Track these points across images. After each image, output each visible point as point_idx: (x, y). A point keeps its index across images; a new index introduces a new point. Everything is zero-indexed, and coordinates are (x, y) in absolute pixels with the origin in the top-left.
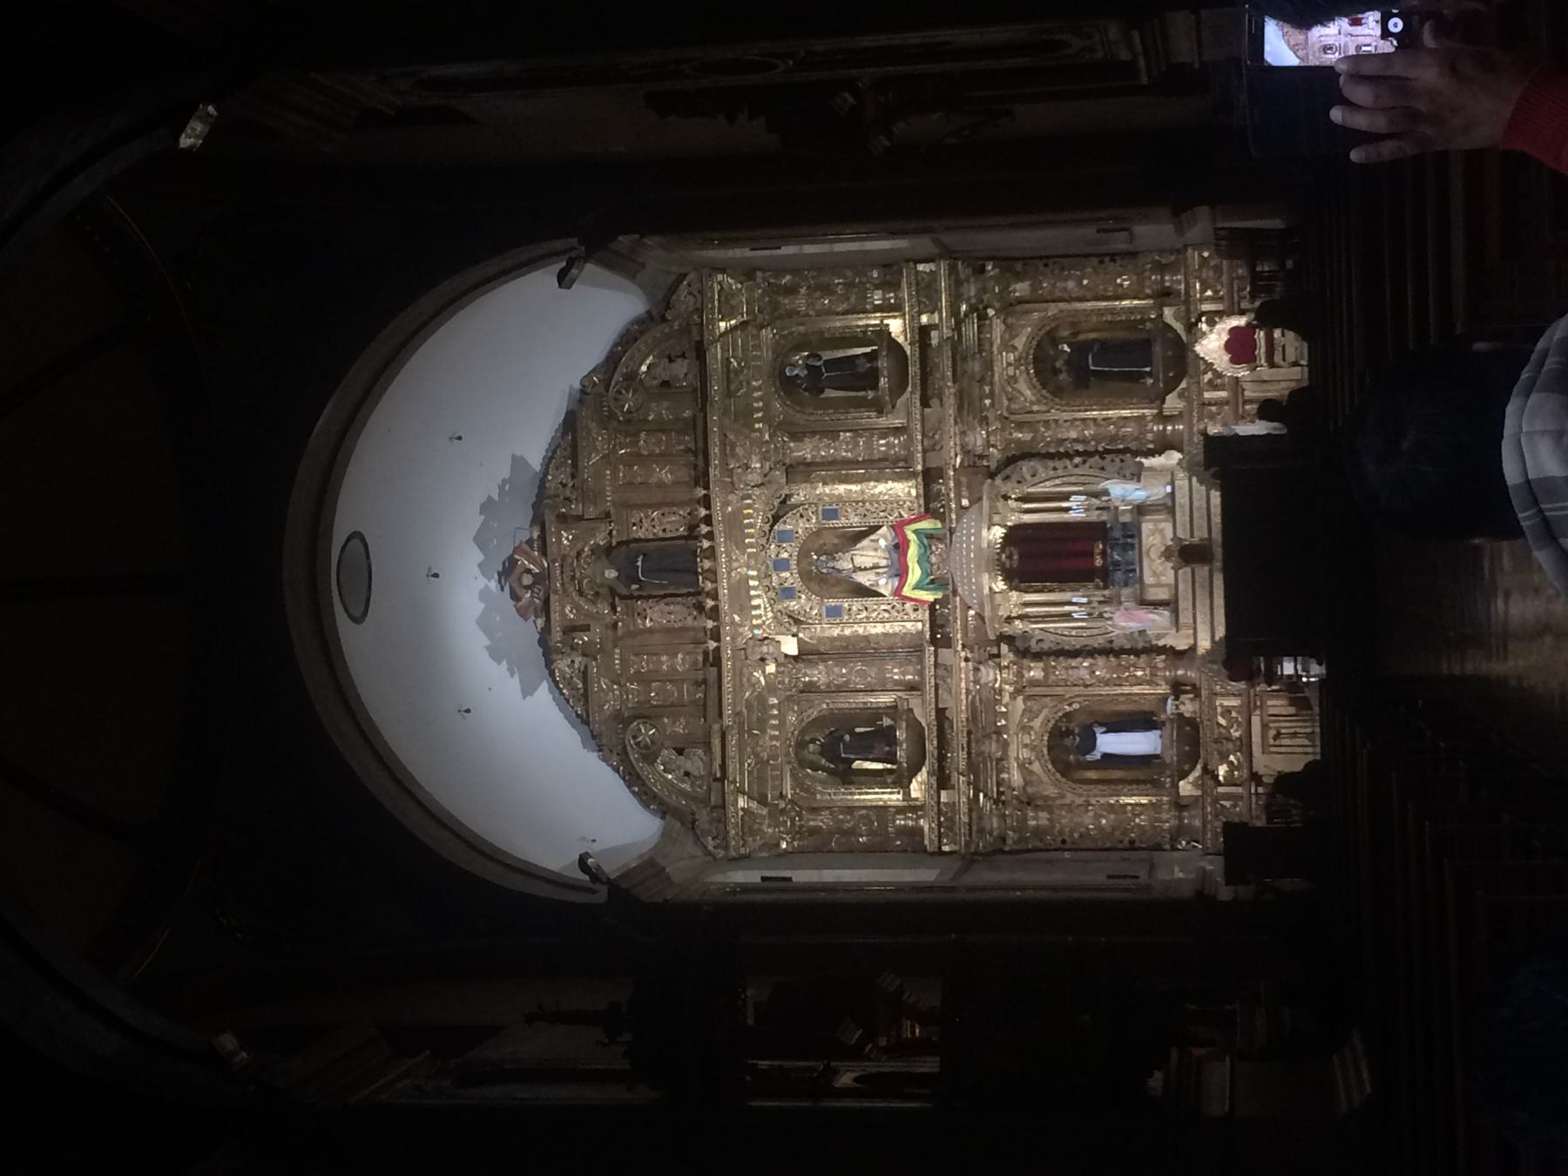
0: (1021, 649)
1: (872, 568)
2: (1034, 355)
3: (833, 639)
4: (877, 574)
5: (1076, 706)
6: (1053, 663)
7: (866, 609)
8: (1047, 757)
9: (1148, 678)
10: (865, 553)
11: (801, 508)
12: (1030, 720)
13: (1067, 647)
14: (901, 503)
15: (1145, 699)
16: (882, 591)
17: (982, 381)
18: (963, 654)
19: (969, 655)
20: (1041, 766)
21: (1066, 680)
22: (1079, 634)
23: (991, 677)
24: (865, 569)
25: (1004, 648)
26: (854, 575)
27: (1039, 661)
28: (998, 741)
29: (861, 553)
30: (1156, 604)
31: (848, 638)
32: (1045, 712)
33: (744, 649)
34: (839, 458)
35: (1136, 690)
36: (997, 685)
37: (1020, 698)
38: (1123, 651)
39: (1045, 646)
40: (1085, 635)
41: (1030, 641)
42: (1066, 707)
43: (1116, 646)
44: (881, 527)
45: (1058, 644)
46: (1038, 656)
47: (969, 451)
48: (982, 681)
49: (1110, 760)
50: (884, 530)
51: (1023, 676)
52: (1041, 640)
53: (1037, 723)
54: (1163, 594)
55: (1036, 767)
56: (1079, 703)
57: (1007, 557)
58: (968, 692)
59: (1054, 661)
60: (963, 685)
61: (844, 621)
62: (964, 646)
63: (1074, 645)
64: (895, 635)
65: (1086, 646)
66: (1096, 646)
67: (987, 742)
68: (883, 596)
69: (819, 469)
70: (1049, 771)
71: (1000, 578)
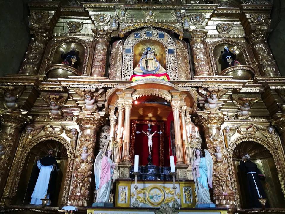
0: (103, 128)
2: (253, 141)
3: (116, 53)
4: (144, 67)
5: (69, 155)
6: (91, 140)
8: (46, 139)
10: (154, 63)
11: (173, 41)
12: (66, 131)
14: (177, 76)
16: (137, 68)
17: (237, 116)
18: (100, 87)
19: (100, 92)
20: (42, 136)
24: (146, 63)
25: (102, 114)
28: (57, 114)
30: (114, 191)
31: (116, 57)
32: (69, 140)
33: (115, 15)
34: (195, 56)
37: (77, 127)
39: (103, 140)
41: (106, 132)
42: (70, 150)
44: (166, 69)
45: (103, 146)
46: (98, 133)
47: (206, 101)
49: (37, 172)
52: (106, 138)
53: (64, 135)
54: (122, 199)
55: (43, 133)
56: (71, 157)
57: (150, 118)
59: (93, 141)
61: (124, 54)
64: (116, 74)
67: (57, 107)
68: (134, 69)
69: (189, 53)
70: (38, 140)
71: (141, 96)
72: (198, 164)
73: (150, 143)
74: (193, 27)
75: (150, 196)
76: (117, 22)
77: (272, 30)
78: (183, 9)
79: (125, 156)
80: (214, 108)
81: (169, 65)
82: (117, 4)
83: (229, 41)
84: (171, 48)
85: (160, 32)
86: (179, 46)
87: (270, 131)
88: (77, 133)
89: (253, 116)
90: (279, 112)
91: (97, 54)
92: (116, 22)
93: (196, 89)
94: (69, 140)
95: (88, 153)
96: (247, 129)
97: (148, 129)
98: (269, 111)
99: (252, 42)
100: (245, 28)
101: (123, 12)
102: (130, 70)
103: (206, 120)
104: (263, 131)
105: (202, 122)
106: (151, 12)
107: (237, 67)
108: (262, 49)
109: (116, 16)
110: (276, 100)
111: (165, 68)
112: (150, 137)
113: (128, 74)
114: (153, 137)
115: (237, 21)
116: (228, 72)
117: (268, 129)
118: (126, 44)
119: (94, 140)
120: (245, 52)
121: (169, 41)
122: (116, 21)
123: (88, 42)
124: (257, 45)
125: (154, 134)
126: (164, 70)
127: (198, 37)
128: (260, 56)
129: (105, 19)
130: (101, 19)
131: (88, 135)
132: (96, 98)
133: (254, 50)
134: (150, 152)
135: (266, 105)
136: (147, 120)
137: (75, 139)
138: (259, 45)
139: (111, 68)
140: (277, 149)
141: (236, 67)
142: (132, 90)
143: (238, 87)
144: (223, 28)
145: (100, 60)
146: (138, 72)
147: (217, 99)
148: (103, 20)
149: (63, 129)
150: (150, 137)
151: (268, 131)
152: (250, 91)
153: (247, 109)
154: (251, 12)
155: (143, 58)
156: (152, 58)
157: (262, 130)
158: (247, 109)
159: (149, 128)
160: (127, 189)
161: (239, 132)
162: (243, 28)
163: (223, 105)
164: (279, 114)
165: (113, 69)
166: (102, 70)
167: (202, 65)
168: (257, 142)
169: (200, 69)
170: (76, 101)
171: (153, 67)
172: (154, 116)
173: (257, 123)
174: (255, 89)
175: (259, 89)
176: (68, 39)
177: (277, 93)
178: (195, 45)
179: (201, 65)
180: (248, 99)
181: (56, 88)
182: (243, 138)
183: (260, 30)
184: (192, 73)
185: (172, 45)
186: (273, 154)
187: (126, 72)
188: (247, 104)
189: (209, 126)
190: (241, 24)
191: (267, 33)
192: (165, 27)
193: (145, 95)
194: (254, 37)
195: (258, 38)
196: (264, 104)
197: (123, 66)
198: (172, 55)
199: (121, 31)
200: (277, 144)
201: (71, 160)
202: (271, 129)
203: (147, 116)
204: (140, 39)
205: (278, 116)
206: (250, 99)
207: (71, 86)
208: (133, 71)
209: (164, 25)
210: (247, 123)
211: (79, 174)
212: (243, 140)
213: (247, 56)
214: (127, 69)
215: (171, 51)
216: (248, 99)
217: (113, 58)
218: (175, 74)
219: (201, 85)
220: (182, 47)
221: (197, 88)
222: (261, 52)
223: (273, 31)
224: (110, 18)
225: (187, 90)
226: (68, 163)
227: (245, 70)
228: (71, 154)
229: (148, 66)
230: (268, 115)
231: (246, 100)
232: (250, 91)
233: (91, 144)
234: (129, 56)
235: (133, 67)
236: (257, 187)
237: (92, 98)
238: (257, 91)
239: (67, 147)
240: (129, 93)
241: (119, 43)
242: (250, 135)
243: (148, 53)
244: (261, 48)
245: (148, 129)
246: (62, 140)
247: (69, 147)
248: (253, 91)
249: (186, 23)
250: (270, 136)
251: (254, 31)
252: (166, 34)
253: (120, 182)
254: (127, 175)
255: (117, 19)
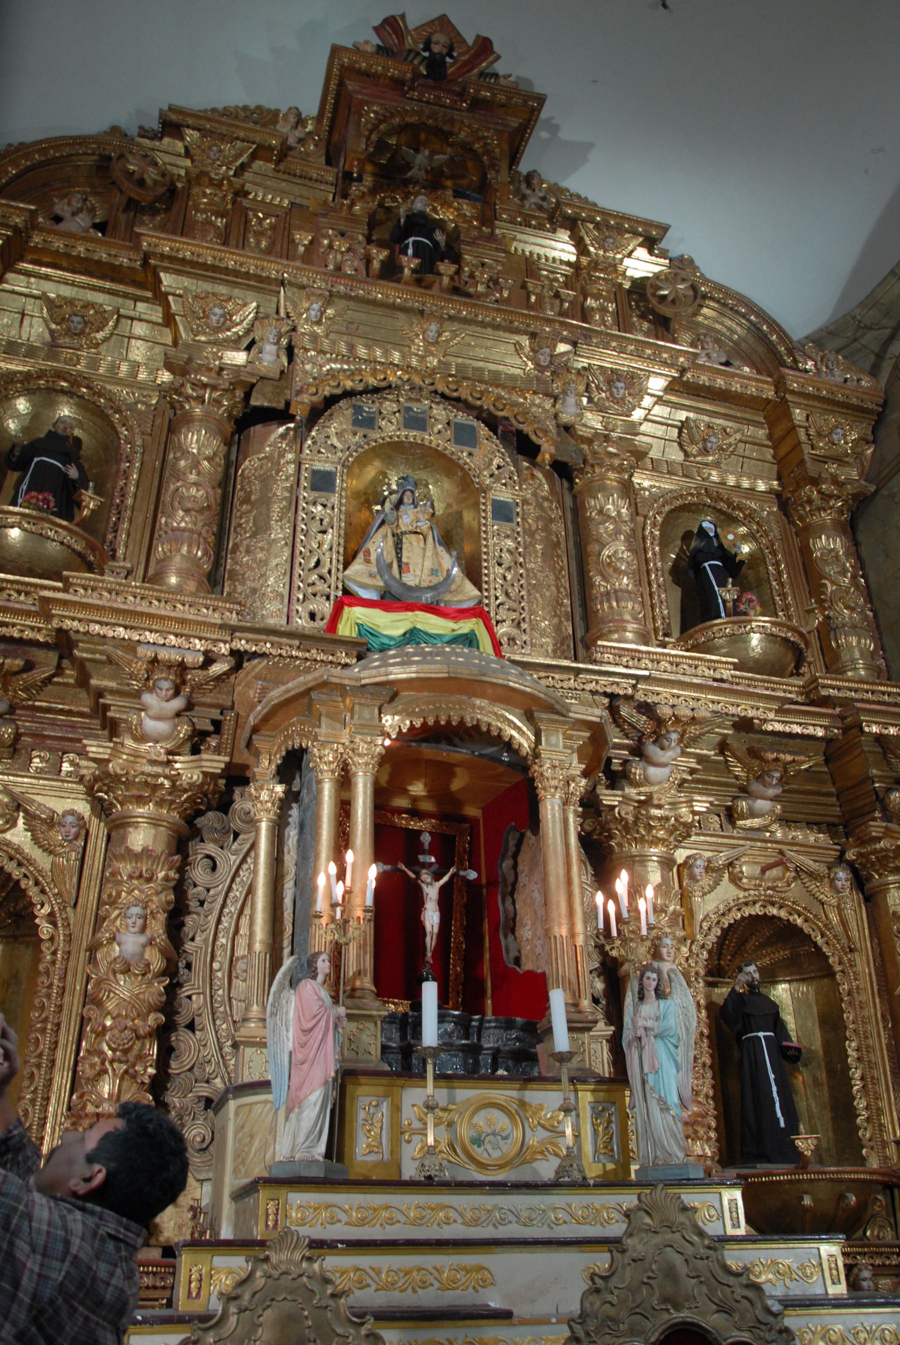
0: (200, 822)
1: (399, 560)
2: (780, 919)
3: (266, 481)
4: (390, 566)
5: (45, 930)
6: (161, 875)
7: (324, 532)
9: (90, 1108)
12: (30, 817)
13: (189, 920)
15: (33, 1101)
16: (357, 567)
19: (217, 668)
21: (113, 903)
22: (218, 952)
23: (152, 726)
24: (398, 548)
25: (214, 762)
26: (386, 529)
27: (169, 843)
29: (429, 553)
31: (266, 501)
32: (43, 861)
33: (278, 312)
34: (593, 548)
35: (62, 1080)
36: (129, 742)
37: (83, 807)
38: (167, 1052)
39: (199, 873)
40: (216, 965)
41: (215, 841)
42: (46, 910)
43: (183, 1039)
45: (202, 903)
47: (638, 751)
48: (148, 698)
50: (473, 591)
51: (140, 800)
52: (214, 868)
56: (52, 939)
57: (415, 799)
58: (131, 646)
59: (166, 879)
60: (151, 637)
62: (239, 658)
63: (193, 939)
65: (189, 966)
66: (185, 991)
68: (345, 568)
69: (569, 525)
72: (650, 1024)
73: (431, 918)
74: (594, 421)
75: (473, 1133)
76: (284, 342)
77: (872, 488)
78: (564, 340)
79: (359, 973)
80: (660, 783)
81: (493, 573)
82: (297, 268)
83: (718, 498)
84: (504, 495)
85: (461, 417)
86: (535, 494)
87: (839, 884)
88: (83, 832)
89: (786, 821)
90: (877, 814)
91: (179, 475)
92: (277, 343)
93: (606, 701)
94: (43, 861)
95: (148, 933)
96: (763, 871)
97: (421, 858)
98: (840, 806)
99: (801, 518)
100: (782, 459)
101: (315, 306)
102: (330, 572)
103: (627, 828)
104: (816, 879)
105: (609, 830)
106: (434, 327)
107: (754, 624)
108: (837, 557)
109: (282, 313)
110: (874, 771)
111: (477, 584)
112: (431, 892)
113: (321, 587)
114: (442, 890)
115: (757, 424)
116: (717, 635)
117: (832, 875)
118: (315, 448)
119: (172, 874)
120: (774, 553)
121: (496, 462)
122: (280, 336)
123: (136, 403)
124: (820, 538)
125: (446, 879)
126: (471, 590)
127: (612, 468)
128: (826, 582)
129: (231, 319)
130: (214, 318)
131: (146, 852)
132: (192, 692)
133: (806, 551)
134: (429, 954)
135: (834, 783)
136: (399, 811)
137: (76, 860)
138: (828, 539)
139: (236, 547)
140: (851, 950)
141: (750, 621)
142: (386, 693)
143: (759, 713)
144: (705, 440)
145: (197, 507)
146: (364, 586)
147: (679, 750)
148: (224, 323)
149: (18, 807)
150: (431, 892)
151: (832, 881)
152: (794, 731)
153: (771, 792)
154: (811, 403)
155: (383, 522)
156: (424, 526)
157: (812, 875)
158: (771, 792)
159: (423, 852)
160: (385, 1107)
161: (735, 880)
162: (774, 457)
163: (692, 771)
164: (876, 827)
165: (248, 552)
166: (203, 555)
167: (621, 590)
168: (791, 918)
169: (611, 607)
170: (100, 693)
171: (426, 571)
172: (432, 795)
173: (797, 848)
174: (814, 725)
175: (826, 728)
176: (39, 377)
177: (882, 747)
178: (595, 497)
179: (616, 591)
180: (782, 756)
181: (14, 625)
182: (746, 904)
183: (835, 481)
184: (577, 618)
185: (505, 485)
186: (838, 968)
187: (314, 577)
188: (777, 775)
189: (634, 849)
190: (770, 437)
191: (855, 496)
192: (486, 404)
193: (437, 722)
194: (810, 501)
195: (825, 510)
196: (828, 777)
197: (299, 548)
198: (507, 528)
199: (299, 392)
200: (854, 933)
201: (54, 953)
202: (841, 874)
203: (405, 792)
204: (375, 435)
205: (874, 834)
206: (789, 758)
207: (96, 628)
208: (340, 575)
209: (481, 392)
210: (763, 845)
211: (108, 1023)
212: (748, 911)
213: (780, 573)
214: (318, 563)
215: (503, 512)
216: (782, 756)
217: (246, 500)
218: (514, 616)
219: (630, 691)
220: (545, 499)
221: (612, 696)
222: (831, 570)
223: (876, 492)
224: (256, 318)
225: (598, 720)
226: (41, 967)
227: (777, 636)
228: (54, 924)
229: (404, 560)
230: (836, 820)
231: (777, 760)
232: (797, 729)
233: (158, 893)
234: (324, 506)
235: (341, 558)
236: (774, 1089)
237: (177, 693)
238: (820, 733)
239: (33, 893)
240: (367, 705)
241: (283, 436)
242: (770, 892)
243: (405, 500)
244: (833, 554)
245: (421, 858)
246: (11, 858)
247: (43, 891)
248: (806, 732)
249: (571, 400)
250: (834, 902)
251: (815, 482)
252: (483, 431)
253: (363, 1079)
254: (372, 1049)
255: (284, 329)
